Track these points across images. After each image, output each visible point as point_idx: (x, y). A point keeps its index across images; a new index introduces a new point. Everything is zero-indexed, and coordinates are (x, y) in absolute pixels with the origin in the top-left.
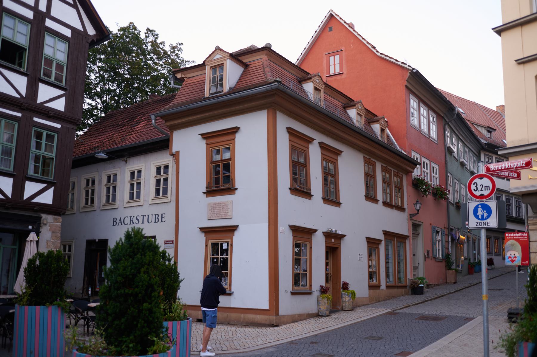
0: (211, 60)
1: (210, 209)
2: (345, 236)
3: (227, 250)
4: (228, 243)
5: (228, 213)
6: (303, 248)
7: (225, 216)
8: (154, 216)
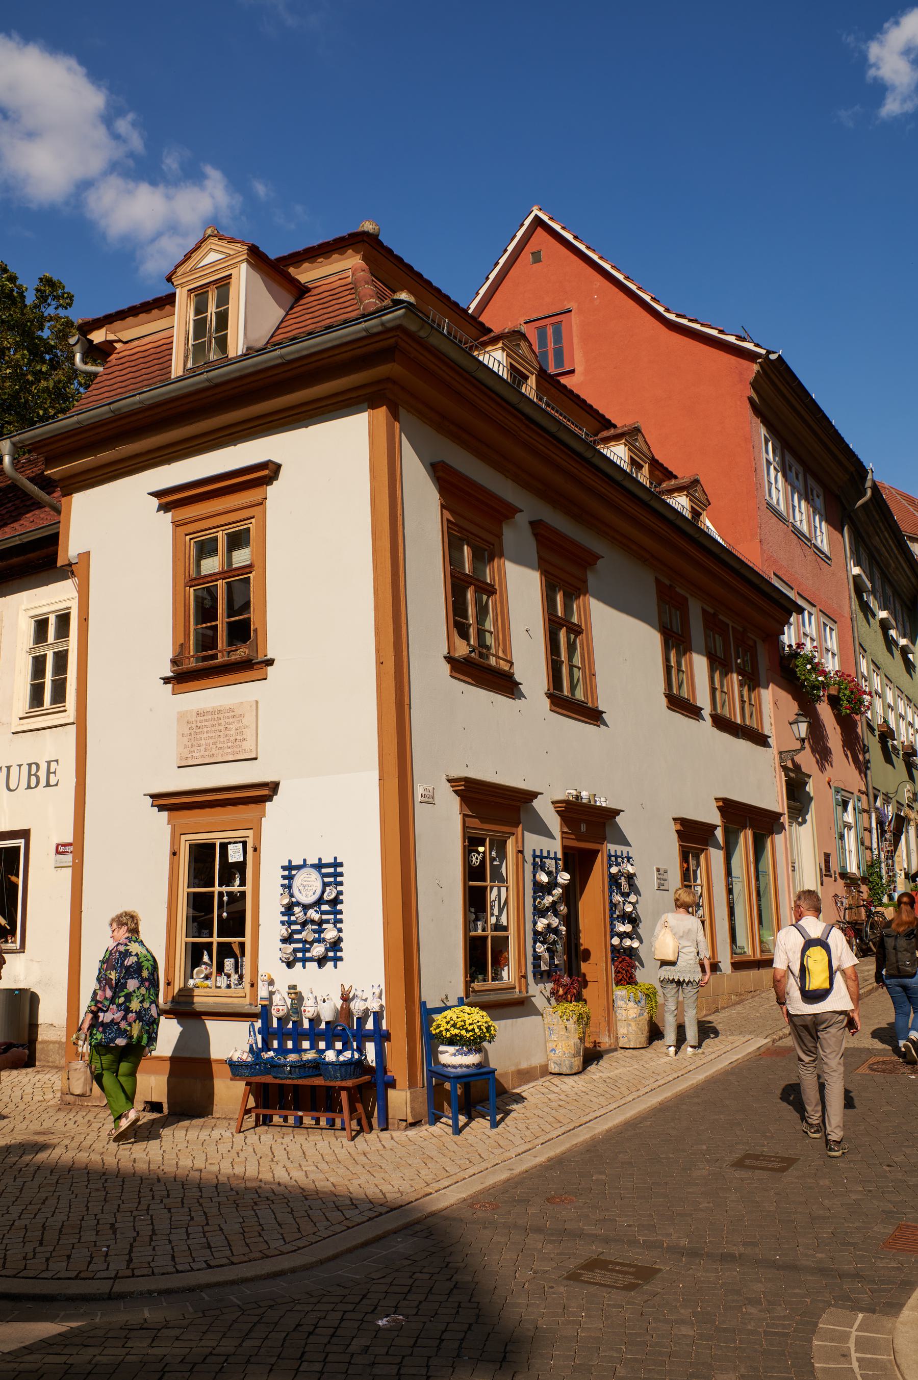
0: (191, 271)
1: (187, 731)
2: (617, 812)
3: (241, 867)
4: (245, 844)
5: (244, 742)
6: (494, 854)
7: (233, 753)
8: (25, 769)
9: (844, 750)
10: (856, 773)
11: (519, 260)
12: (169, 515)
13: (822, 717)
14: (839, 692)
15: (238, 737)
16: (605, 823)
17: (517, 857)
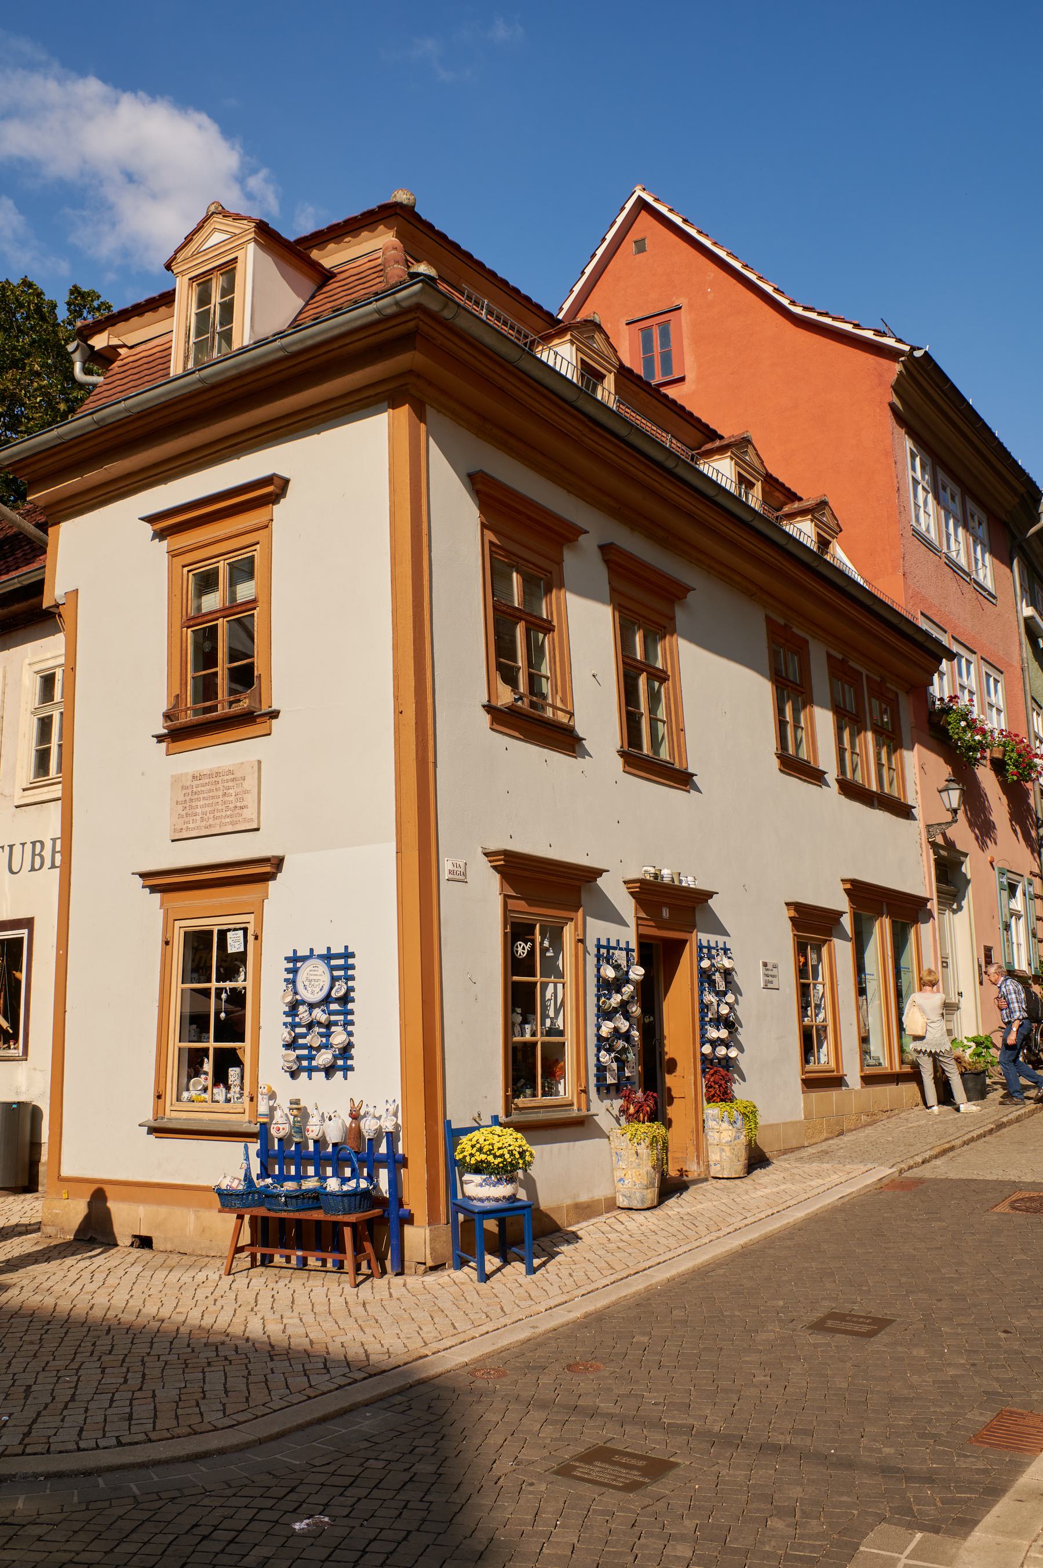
0: (192, 256)
1: (181, 798)
3: (241, 958)
4: (245, 930)
5: (245, 810)
6: (546, 944)
7: (232, 823)
8: (29, 848)
9: (1012, 825)
10: (1028, 851)
11: (619, 250)
12: (165, 542)
13: (983, 785)
14: (1004, 755)
15: (238, 804)
16: (694, 908)
17: (576, 948)
